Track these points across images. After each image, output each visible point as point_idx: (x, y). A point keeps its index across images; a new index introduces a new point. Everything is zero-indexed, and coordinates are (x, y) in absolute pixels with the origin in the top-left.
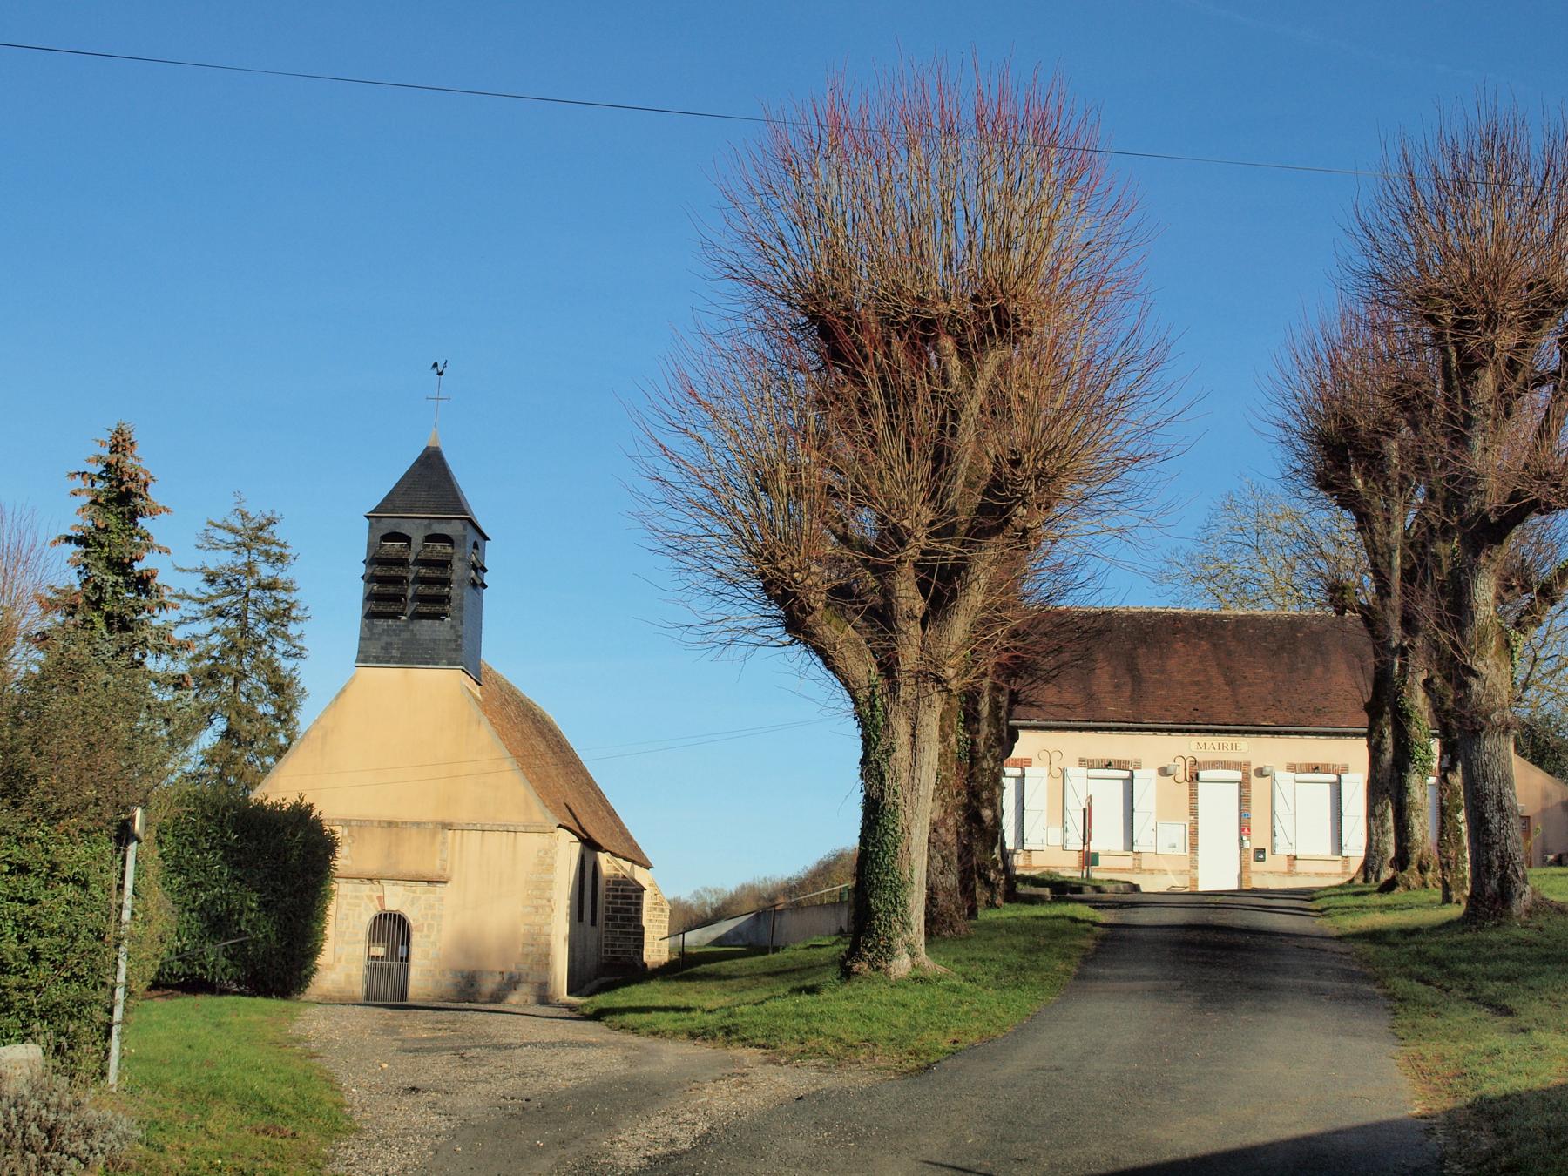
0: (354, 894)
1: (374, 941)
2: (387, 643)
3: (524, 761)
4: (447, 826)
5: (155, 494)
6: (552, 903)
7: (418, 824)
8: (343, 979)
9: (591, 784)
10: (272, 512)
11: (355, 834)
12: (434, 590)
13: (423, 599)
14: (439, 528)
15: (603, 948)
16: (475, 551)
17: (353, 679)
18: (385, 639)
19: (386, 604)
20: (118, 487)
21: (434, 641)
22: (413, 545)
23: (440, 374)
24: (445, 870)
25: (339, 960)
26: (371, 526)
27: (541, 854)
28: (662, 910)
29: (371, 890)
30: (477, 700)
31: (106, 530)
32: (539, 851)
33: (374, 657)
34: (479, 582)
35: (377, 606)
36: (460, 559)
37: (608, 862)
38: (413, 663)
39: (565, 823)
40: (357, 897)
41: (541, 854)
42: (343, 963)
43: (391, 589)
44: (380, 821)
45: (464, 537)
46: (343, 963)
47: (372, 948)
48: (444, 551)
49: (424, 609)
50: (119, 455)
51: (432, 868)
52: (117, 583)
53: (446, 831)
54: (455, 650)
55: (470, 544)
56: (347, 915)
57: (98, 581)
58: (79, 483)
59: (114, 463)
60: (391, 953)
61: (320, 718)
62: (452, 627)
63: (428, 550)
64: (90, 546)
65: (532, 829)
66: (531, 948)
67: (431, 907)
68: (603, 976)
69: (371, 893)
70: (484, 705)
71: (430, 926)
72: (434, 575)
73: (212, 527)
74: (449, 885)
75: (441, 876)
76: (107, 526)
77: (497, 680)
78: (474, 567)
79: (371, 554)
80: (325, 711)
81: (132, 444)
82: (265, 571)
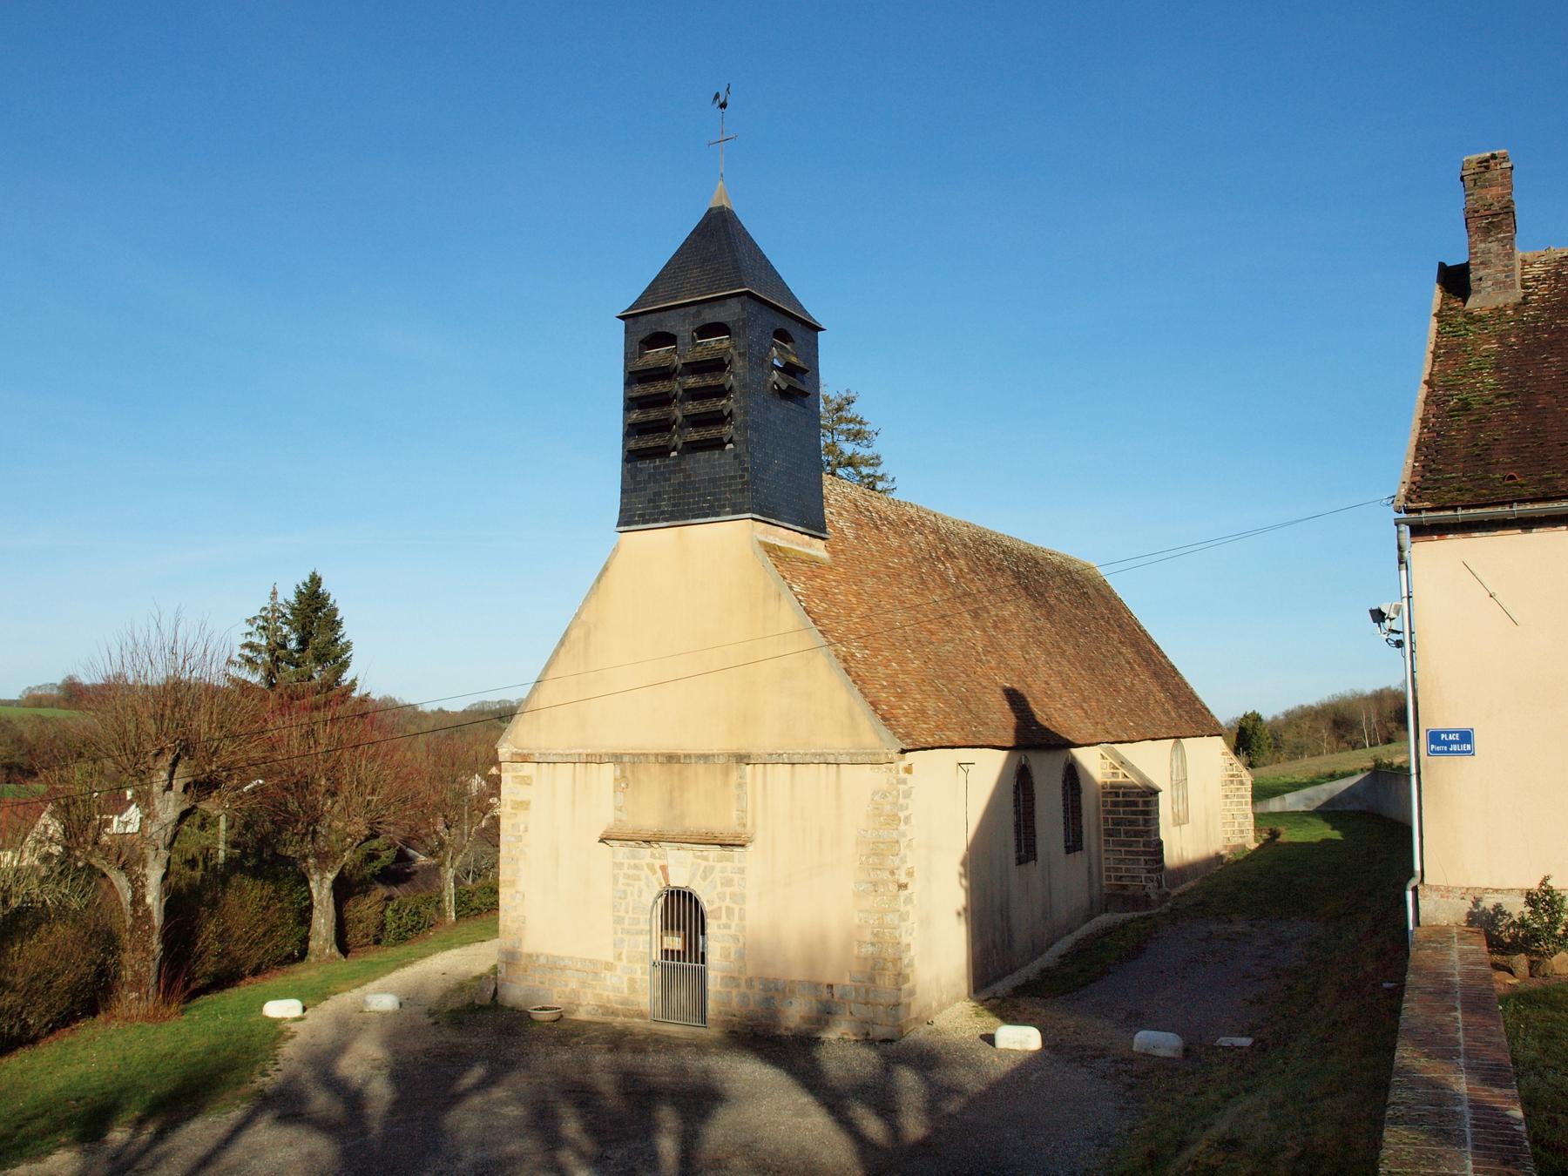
0: (633, 862)
1: (667, 929)
4: (742, 759)
7: (705, 758)
8: (625, 985)
10: (848, 391)
11: (628, 774)
13: (696, 421)
14: (711, 315)
17: (616, 550)
21: (713, 481)
23: (723, 106)
24: (745, 826)
25: (619, 957)
28: (1242, 783)
29: (653, 856)
32: (874, 793)
33: (640, 515)
35: (638, 441)
37: (1103, 757)
40: (636, 867)
42: (625, 961)
43: (654, 414)
44: (657, 755)
46: (625, 961)
47: (665, 938)
49: (694, 435)
51: (724, 822)
53: (743, 766)
54: (742, 490)
56: (625, 892)
61: (581, 609)
62: (736, 456)
63: (699, 349)
65: (860, 759)
67: (728, 882)
68: (1106, 911)
74: (751, 848)
75: (738, 836)
80: (587, 600)
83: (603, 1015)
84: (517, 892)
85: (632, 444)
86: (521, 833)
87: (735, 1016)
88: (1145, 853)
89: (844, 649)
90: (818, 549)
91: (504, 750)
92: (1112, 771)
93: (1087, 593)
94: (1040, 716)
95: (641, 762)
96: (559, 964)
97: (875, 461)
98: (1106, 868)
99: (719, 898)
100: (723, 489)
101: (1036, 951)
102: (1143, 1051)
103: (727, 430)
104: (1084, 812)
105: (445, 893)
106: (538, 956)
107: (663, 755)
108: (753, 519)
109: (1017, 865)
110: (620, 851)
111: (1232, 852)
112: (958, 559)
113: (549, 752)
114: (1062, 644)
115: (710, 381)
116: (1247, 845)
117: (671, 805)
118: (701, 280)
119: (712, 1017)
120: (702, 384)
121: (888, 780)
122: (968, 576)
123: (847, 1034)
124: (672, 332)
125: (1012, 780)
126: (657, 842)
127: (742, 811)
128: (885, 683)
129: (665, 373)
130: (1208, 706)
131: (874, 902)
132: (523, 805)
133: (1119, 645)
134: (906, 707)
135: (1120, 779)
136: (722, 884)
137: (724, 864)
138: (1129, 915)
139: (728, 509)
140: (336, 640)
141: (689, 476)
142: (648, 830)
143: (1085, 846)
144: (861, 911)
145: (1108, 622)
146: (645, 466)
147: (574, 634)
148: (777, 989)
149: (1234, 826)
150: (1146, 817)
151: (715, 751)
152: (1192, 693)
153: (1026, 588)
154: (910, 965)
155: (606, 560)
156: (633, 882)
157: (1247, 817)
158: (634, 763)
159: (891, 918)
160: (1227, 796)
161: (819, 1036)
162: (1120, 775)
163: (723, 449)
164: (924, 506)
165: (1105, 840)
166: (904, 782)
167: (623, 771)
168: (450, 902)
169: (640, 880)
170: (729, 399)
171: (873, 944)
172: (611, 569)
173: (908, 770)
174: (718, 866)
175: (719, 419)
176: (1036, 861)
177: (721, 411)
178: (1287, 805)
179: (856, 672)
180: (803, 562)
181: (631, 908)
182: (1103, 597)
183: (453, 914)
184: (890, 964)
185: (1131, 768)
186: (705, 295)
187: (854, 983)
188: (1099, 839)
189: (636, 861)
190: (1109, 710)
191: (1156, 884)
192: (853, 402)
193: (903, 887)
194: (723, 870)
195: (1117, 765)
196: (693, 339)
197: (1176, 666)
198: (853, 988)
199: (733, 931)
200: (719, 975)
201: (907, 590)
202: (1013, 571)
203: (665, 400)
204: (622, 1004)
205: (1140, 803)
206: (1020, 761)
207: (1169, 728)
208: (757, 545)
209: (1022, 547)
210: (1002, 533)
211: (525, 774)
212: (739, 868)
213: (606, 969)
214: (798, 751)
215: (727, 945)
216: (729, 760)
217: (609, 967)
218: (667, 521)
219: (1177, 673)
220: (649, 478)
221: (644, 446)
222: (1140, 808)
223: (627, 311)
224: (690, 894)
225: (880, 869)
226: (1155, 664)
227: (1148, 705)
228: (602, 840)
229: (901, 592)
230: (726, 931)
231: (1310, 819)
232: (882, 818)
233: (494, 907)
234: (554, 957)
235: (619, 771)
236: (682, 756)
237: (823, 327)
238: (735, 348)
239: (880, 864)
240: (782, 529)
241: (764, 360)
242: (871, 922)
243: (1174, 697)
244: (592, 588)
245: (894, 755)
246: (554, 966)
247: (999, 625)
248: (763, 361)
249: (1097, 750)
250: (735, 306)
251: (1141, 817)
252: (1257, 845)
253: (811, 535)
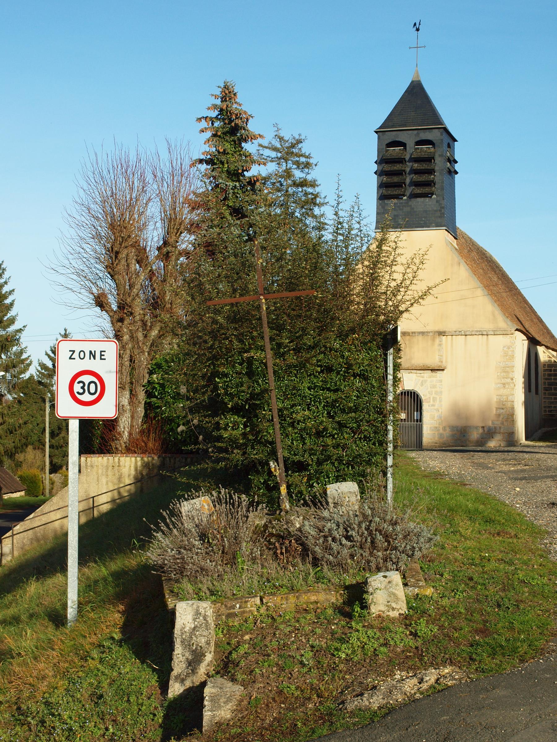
3: (488, 287)
4: (441, 333)
5: (252, 127)
6: (514, 381)
7: (423, 333)
9: (525, 301)
12: (423, 178)
13: (417, 184)
16: (448, 149)
20: (229, 124)
21: (426, 211)
23: (418, 30)
24: (442, 362)
26: (379, 138)
30: (456, 249)
31: (225, 153)
32: (504, 347)
34: (452, 170)
36: (440, 156)
38: (413, 228)
39: (519, 328)
43: (396, 179)
45: (442, 140)
49: (418, 191)
50: (228, 103)
51: (433, 361)
52: (235, 187)
53: (442, 337)
54: (440, 217)
55: (445, 145)
57: (223, 186)
58: (204, 124)
59: (224, 108)
60: (410, 417)
62: (437, 202)
64: (215, 164)
65: (498, 333)
66: (502, 411)
67: (434, 387)
70: (460, 251)
71: (434, 399)
72: (423, 168)
73: (261, 148)
74: (445, 371)
76: (224, 150)
77: (464, 236)
78: (449, 160)
79: (380, 157)
81: (235, 94)
82: (298, 174)
97: (313, 184)
108: (446, 230)
120: (422, 168)
124: (404, 141)
171: (503, 409)
175: (430, 184)
192: (301, 142)
199: (436, 407)
221: (392, 193)
224: (414, 393)
230: (432, 407)
245: (513, 331)
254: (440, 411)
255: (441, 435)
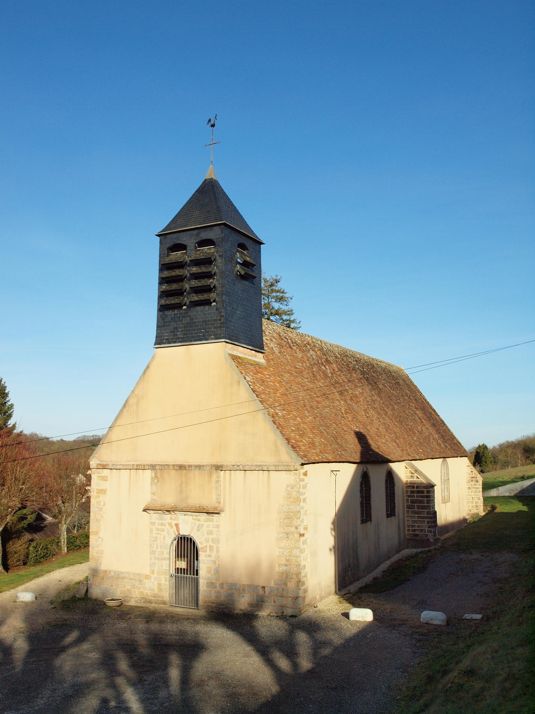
0: (161, 522)
1: (178, 557)
2: (174, 328)
4: (219, 468)
10: (276, 276)
11: (159, 475)
13: (197, 290)
15: (407, 528)
17: (153, 358)
18: (174, 325)
19: (172, 298)
21: (205, 322)
22: (189, 252)
23: (213, 126)
24: (220, 503)
25: (153, 572)
27: (289, 489)
28: (477, 481)
29: (171, 518)
32: (288, 486)
33: (166, 339)
35: (165, 300)
37: (406, 468)
38: (191, 341)
40: (162, 524)
41: (289, 489)
42: (156, 575)
43: (174, 286)
44: (174, 465)
48: (209, 251)
49: (195, 298)
51: (209, 502)
53: (219, 471)
54: (220, 327)
56: (156, 538)
61: (135, 388)
62: (217, 309)
63: (198, 253)
65: (280, 468)
67: (210, 533)
69: (171, 521)
74: (223, 514)
75: (216, 508)
80: (137, 384)
83: (144, 603)
84: (99, 538)
85: (163, 302)
86: (100, 507)
87: (213, 603)
88: (427, 518)
89: (272, 411)
90: (259, 358)
91: (93, 462)
92: (411, 475)
93: (399, 382)
94: (374, 446)
95: (165, 469)
96: (121, 576)
97: (290, 313)
98: (407, 525)
99: (206, 541)
100: (210, 326)
101: (371, 568)
102: (425, 621)
103: (213, 295)
104: (396, 496)
105: (62, 538)
106: (110, 572)
107: (177, 465)
108: (225, 342)
109: (361, 524)
110: (154, 516)
111: (472, 517)
112: (333, 364)
113: (117, 463)
114: (386, 409)
115: (204, 269)
116: (480, 514)
117: (181, 492)
118: (200, 216)
119: (201, 604)
120: (200, 271)
121: (295, 479)
122: (338, 373)
123: (272, 613)
125: (359, 480)
126: (174, 511)
127: (218, 495)
128: (294, 429)
129: (180, 265)
130: (460, 442)
131: (287, 544)
132: (103, 492)
133: (415, 409)
134: (304, 441)
135: (415, 479)
136: (207, 533)
137: (208, 523)
138: (419, 550)
139: (212, 337)
140: (5, 403)
141: (192, 319)
142: (169, 505)
143: (396, 514)
144: (280, 548)
145: (409, 397)
146: (170, 313)
147: (131, 401)
148: (236, 589)
149: (473, 503)
150: (428, 499)
151: (204, 464)
152: (452, 434)
153: (367, 379)
154: (305, 576)
155: (148, 363)
156: (159, 532)
157: (479, 499)
158: (162, 469)
159: (296, 552)
160: (469, 488)
161: (257, 614)
162: (415, 477)
163: (211, 305)
164: (315, 337)
165: (407, 511)
166: (303, 480)
167: (156, 474)
168: (64, 542)
169: (164, 531)
170: (214, 279)
171: (286, 565)
172: (151, 367)
173: (305, 474)
174: (206, 524)
175: (208, 289)
176: (371, 521)
177: (210, 285)
178: (500, 492)
179: (279, 423)
180: (252, 365)
181: (159, 546)
182: (407, 384)
183: (66, 549)
184: (295, 576)
185: (421, 473)
186: (202, 224)
187: (275, 586)
188: (404, 510)
189: (162, 522)
190: (410, 443)
191: (433, 534)
192: (279, 281)
193: (302, 535)
194: (208, 526)
195: (413, 472)
196: (196, 248)
197: (444, 421)
198: (275, 588)
199: (213, 559)
200: (205, 581)
201: (306, 380)
202: (361, 370)
203: (180, 279)
204: (154, 597)
205: (425, 491)
206: (363, 469)
207: (440, 452)
208: (228, 356)
209: (365, 358)
210: (355, 351)
211: (104, 475)
212: (216, 525)
213: (146, 579)
214: (248, 464)
215: (210, 566)
216: (211, 468)
217: (147, 577)
218: (181, 342)
219: (445, 424)
220: (171, 320)
221: (169, 303)
222: (425, 494)
223: (161, 232)
224: (191, 539)
225: (290, 526)
226: (434, 420)
227: (429, 440)
228: (144, 510)
229: (302, 381)
230: (209, 558)
231: (512, 500)
232: (291, 499)
233: (87, 545)
234: (119, 572)
235: (154, 474)
236: (187, 466)
237: (264, 242)
238: (217, 252)
239: (290, 523)
240: (241, 348)
241: (233, 259)
242: (285, 553)
243: (443, 437)
244: (141, 377)
246: (118, 576)
247: (353, 398)
248: (231, 259)
249: (403, 464)
250: (217, 230)
251: (425, 499)
252: (485, 513)
253: (256, 351)
254: (217, 563)
255: (218, 592)
